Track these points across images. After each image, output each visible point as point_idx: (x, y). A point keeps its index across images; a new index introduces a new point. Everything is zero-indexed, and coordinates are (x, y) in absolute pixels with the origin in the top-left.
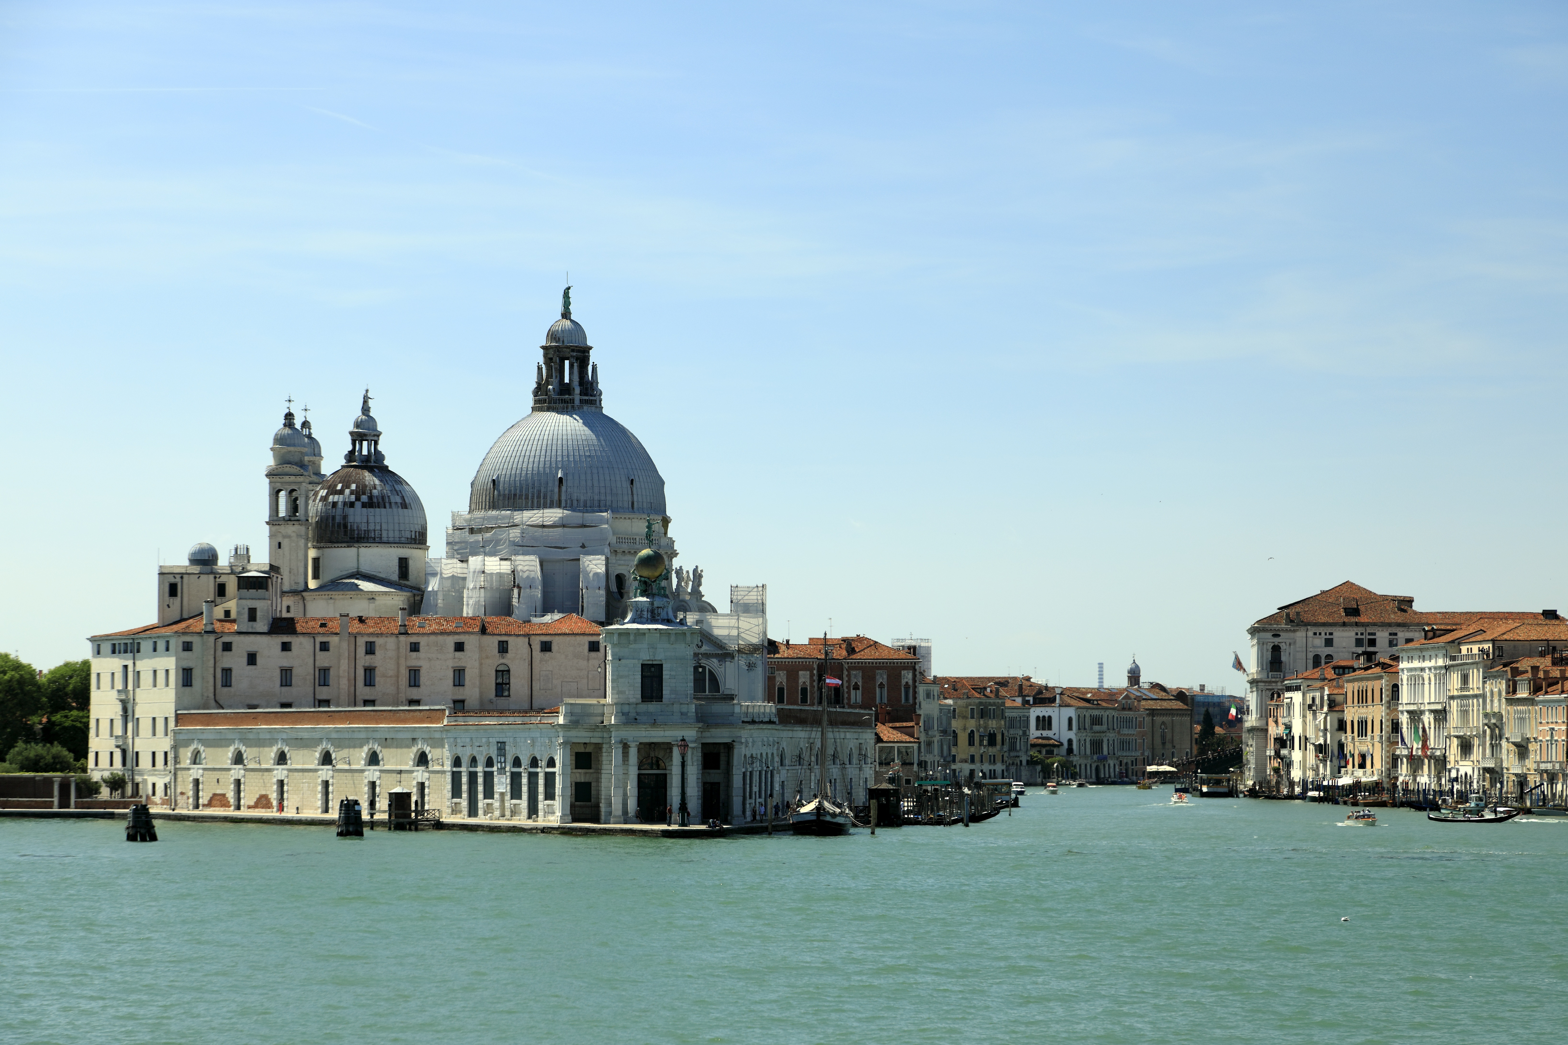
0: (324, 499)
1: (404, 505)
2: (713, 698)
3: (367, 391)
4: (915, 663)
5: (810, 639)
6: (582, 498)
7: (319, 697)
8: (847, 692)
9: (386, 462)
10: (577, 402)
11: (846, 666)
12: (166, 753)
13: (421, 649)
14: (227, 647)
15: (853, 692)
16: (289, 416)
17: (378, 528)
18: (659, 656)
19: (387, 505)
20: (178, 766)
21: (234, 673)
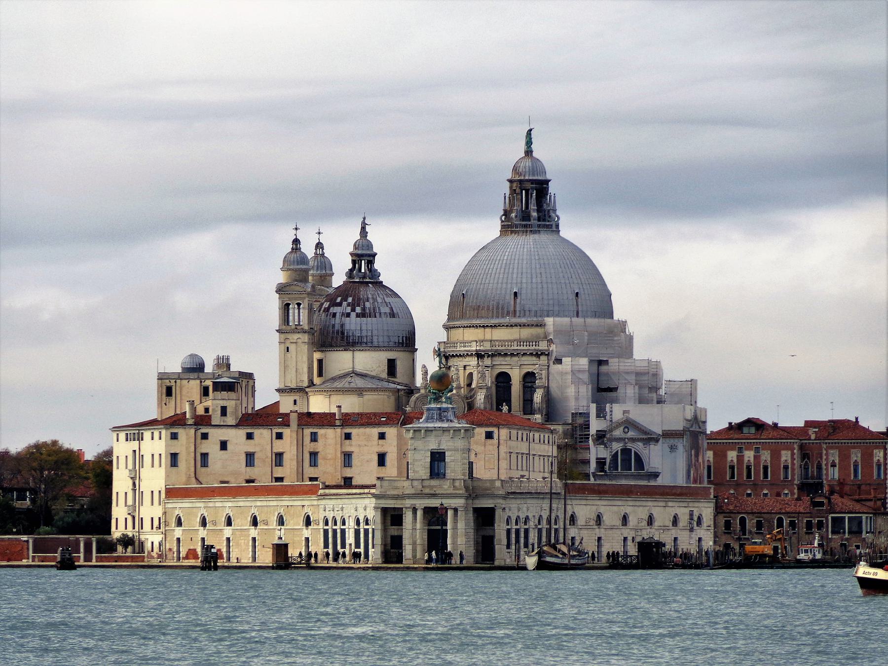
0: (327, 310)
1: (393, 315)
2: (639, 475)
3: (364, 218)
4: (886, 443)
5: (806, 422)
6: (534, 309)
8: (825, 469)
11: (824, 446)
12: (160, 518)
13: (353, 438)
14: (205, 436)
15: (831, 469)
16: (296, 241)
17: (369, 334)
18: (443, 446)
19: (377, 315)
20: (167, 529)
21: (210, 457)
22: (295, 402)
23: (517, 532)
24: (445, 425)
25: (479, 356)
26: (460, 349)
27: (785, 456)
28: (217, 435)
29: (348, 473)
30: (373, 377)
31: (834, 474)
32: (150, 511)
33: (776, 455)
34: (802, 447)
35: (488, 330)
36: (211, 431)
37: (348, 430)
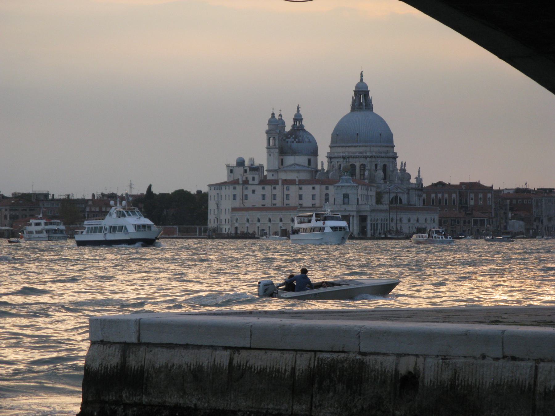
0: (285, 140)
1: (310, 142)
3: (298, 105)
5: (460, 183)
7: (273, 203)
9: (305, 128)
10: (364, 109)
11: (468, 192)
12: (229, 220)
14: (246, 188)
16: (273, 114)
19: (304, 142)
22: (273, 175)
23: (374, 224)
24: (348, 184)
25: (344, 158)
26: (336, 155)
27: (454, 196)
28: (251, 188)
29: (301, 202)
30: (302, 166)
31: (472, 203)
32: (225, 216)
33: (450, 196)
34: (460, 192)
35: (347, 148)
36: (249, 187)
37: (301, 186)
